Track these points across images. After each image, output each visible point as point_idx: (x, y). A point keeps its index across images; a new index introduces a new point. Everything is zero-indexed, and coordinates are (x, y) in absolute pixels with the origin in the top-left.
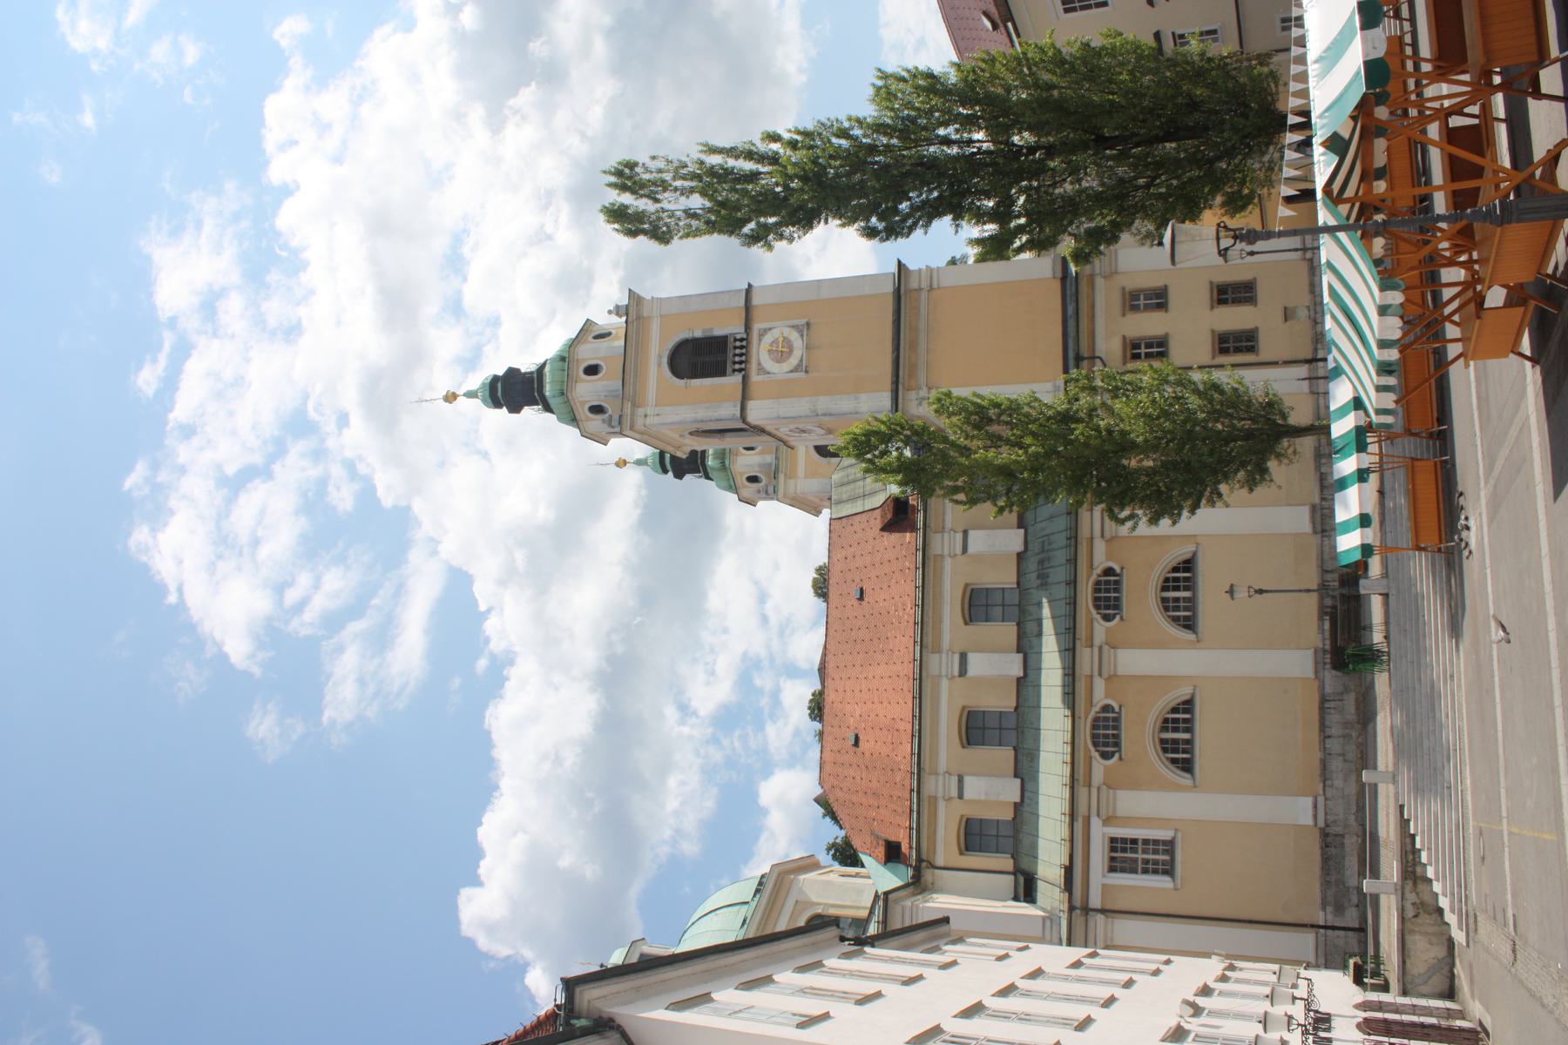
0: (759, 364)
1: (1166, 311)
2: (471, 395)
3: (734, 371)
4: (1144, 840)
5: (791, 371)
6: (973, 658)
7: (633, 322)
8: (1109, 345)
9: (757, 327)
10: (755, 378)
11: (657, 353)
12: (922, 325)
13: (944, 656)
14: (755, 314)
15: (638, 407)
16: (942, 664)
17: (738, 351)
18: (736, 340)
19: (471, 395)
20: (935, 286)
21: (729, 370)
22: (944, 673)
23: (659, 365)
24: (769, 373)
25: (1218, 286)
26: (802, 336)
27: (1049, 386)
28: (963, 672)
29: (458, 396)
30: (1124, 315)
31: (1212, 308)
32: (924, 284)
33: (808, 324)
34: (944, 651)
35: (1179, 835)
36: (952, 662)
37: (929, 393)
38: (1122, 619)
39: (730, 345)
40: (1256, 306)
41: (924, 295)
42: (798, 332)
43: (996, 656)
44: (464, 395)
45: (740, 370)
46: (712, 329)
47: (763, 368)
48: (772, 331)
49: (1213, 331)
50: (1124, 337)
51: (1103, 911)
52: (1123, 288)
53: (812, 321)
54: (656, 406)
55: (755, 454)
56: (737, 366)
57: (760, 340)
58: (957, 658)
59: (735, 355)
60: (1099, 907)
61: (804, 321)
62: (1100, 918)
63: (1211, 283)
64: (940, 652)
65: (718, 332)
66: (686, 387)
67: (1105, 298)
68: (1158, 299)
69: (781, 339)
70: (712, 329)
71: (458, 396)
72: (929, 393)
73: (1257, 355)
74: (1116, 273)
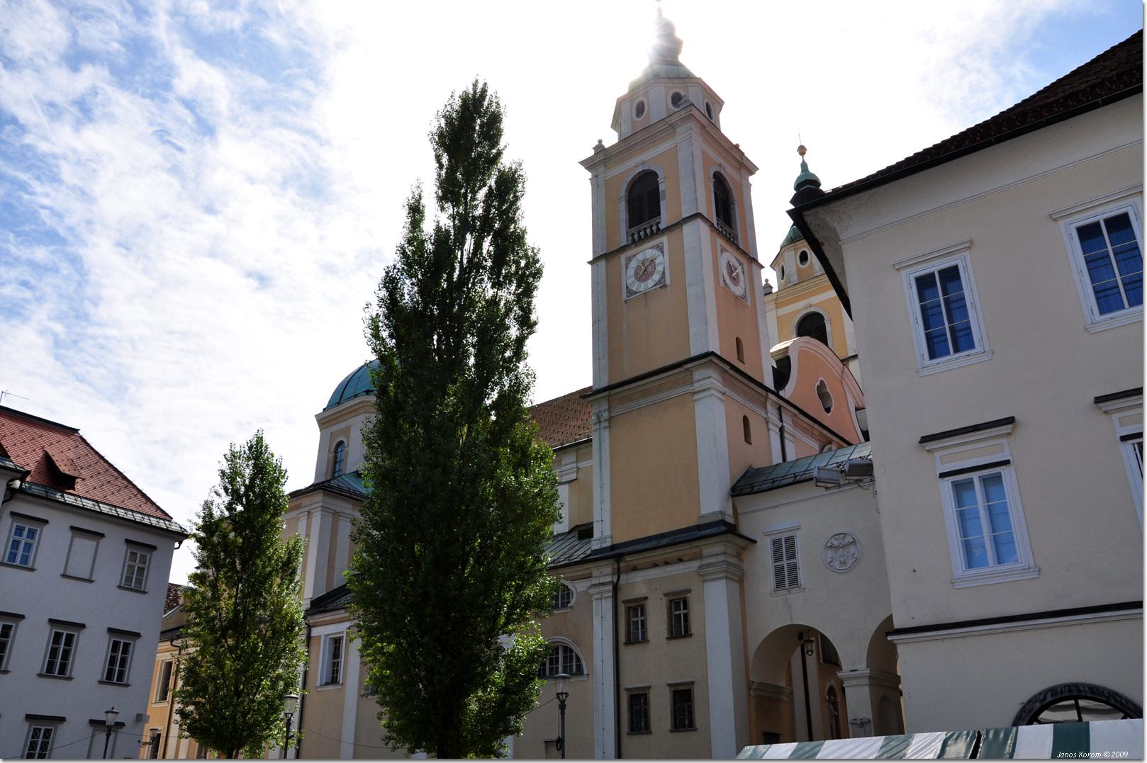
1: (667, 638)
4: (338, 662)
5: (627, 287)
8: (638, 583)
9: (664, 240)
10: (623, 257)
11: (645, 160)
12: (662, 396)
14: (675, 233)
15: (605, 166)
18: (658, 223)
20: (696, 397)
24: (627, 268)
25: (690, 690)
26: (655, 285)
27: (608, 532)
30: (665, 595)
31: (669, 685)
32: (697, 386)
33: (665, 286)
35: (340, 687)
37: (604, 420)
39: (653, 222)
40: (671, 731)
41: (688, 389)
45: (634, 241)
46: (665, 198)
47: (631, 260)
49: (649, 688)
50: (646, 598)
52: (689, 591)
53: (668, 289)
54: (605, 181)
55: (797, 266)
57: (653, 248)
59: (645, 229)
61: (668, 281)
63: (692, 683)
67: (677, 574)
68: (680, 627)
72: (604, 420)
73: (628, 734)
74: (704, 581)
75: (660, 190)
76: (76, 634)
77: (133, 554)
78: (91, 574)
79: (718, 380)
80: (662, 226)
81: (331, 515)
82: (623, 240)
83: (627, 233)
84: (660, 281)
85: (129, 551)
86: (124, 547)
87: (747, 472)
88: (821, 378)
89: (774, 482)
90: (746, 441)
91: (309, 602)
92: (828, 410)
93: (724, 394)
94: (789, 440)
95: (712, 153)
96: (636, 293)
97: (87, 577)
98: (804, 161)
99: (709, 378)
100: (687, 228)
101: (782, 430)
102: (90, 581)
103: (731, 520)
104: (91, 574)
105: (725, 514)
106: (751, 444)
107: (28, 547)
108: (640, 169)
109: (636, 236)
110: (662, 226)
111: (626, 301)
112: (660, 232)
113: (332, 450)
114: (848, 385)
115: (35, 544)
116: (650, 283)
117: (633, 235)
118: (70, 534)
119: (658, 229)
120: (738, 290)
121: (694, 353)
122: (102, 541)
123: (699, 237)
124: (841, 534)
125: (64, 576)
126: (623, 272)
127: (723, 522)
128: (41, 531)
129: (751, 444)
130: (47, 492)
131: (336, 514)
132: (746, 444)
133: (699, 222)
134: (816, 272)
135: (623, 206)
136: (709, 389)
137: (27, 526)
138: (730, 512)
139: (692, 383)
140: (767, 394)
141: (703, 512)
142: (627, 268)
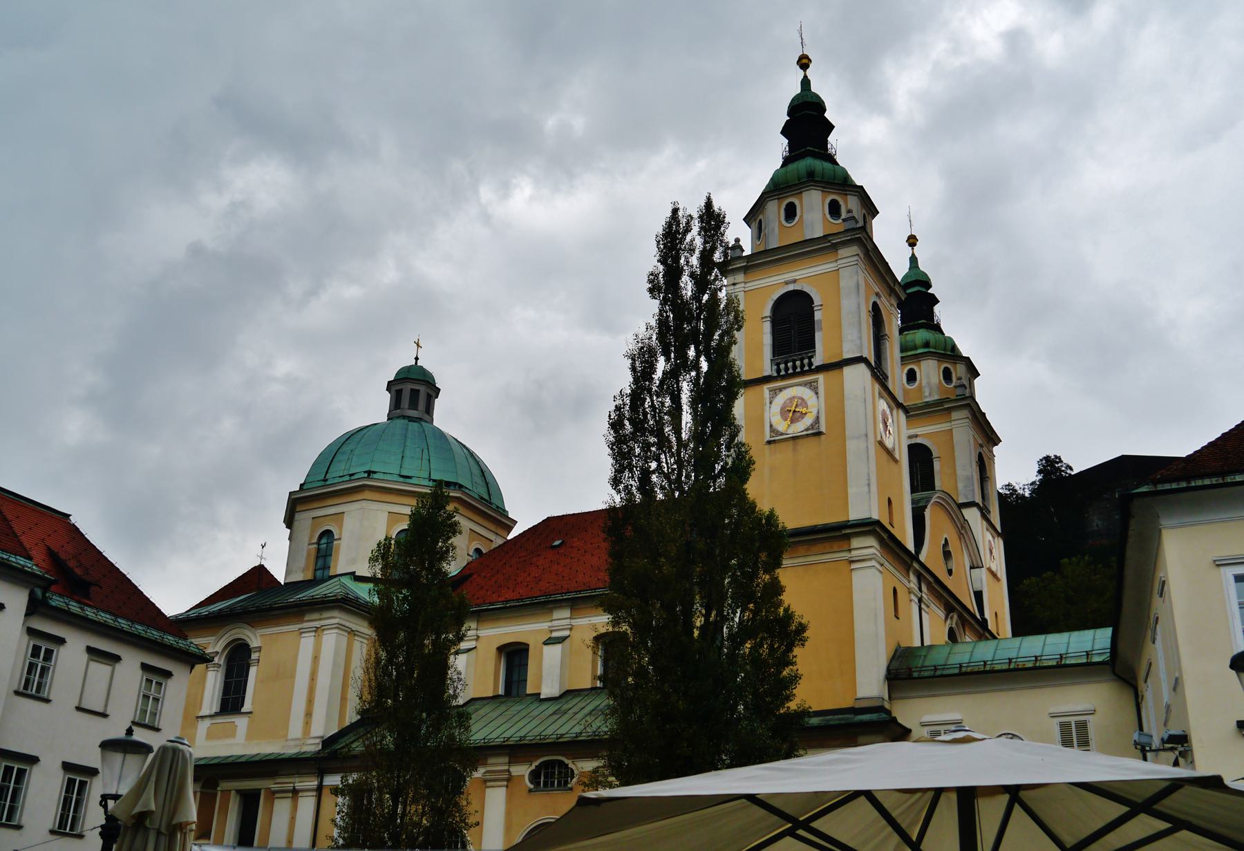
0: (781, 389)
2: (806, 83)
3: (778, 365)
5: (771, 426)
6: (557, 649)
7: (830, 241)
9: (820, 378)
10: (766, 388)
11: (797, 278)
13: (568, 621)
14: (833, 374)
15: (745, 273)
16: (561, 617)
17: (798, 363)
18: (812, 357)
19: (806, 83)
20: (854, 566)
21: (779, 359)
22: (555, 623)
23: (787, 283)
24: (771, 403)
26: (807, 430)
28: (550, 641)
29: (805, 71)
32: (854, 553)
33: (819, 434)
34: (573, 621)
36: (563, 629)
38: (530, 791)
41: (846, 555)
42: (812, 425)
43: (557, 671)
44: (805, 77)
45: (779, 371)
46: (821, 329)
48: (815, 396)
51: (320, 789)
56: (782, 366)
57: (805, 384)
58: (566, 633)
59: (794, 361)
60: (324, 784)
61: (823, 429)
62: (314, 783)
64: (570, 618)
65: (818, 336)
66: (762, 318)
69: (804, 410)
70: (821, 329)
71: (805, 71)
75: (816, 318)
76: (89, 780)
77: (149, 681)
78: (106, 706)
79: (878, 550)
80: (817, 361)
81: (346, 634)
82: (767, 369)
83: (771, 360)
84: (812, 426)
85: (145, 678)
86: (140, 672)
87: (896, 651)
88: (945, 536)
89: (936, 669)
90: (895, 616)
91: (318, 741)
92: (950, 572)
93: (882, 565)
94: (926, 611)
95: (871, 281)
96: (782, 434)
97: (100, 710)
98: (913, 254)
99: (867, 546)
100: (848, 371)
101: (920, 600)
102: (104, 715)
103: (887, 706)
104: (106, 706)
105: (883, 699)
106: (898, 618)
107: (44, 670)
108: (791, 287)
109: (782, 366)
110: (817, 361)
111: (769, 442)
112: (812, 371)
113: (315, 540)
114: (966, 542)
115: (142, 689)
116: (799, 428)
117: (778, 365)
118: (85, 656)
119: (810, 364)
120: (889, 443)
121: (855, 514)
122: (118, 666)
123: (857, 379)
124: (1009, 734)
125: (79, 709)
126: (767, 408)
127: (880, 709)
128: (58, 651)
129: (898, 618)
130: (68, 605)
131: (352, 633)
132: (895, 618)
133: (862, 366)
134: (926, 397)
135: (767, 326)
136: (870, 559)
137: (44, 646)
138: (886, 697)
139: (850, 550)
140: (912, 563)
141: (859, 695)
142: (771, 403)
